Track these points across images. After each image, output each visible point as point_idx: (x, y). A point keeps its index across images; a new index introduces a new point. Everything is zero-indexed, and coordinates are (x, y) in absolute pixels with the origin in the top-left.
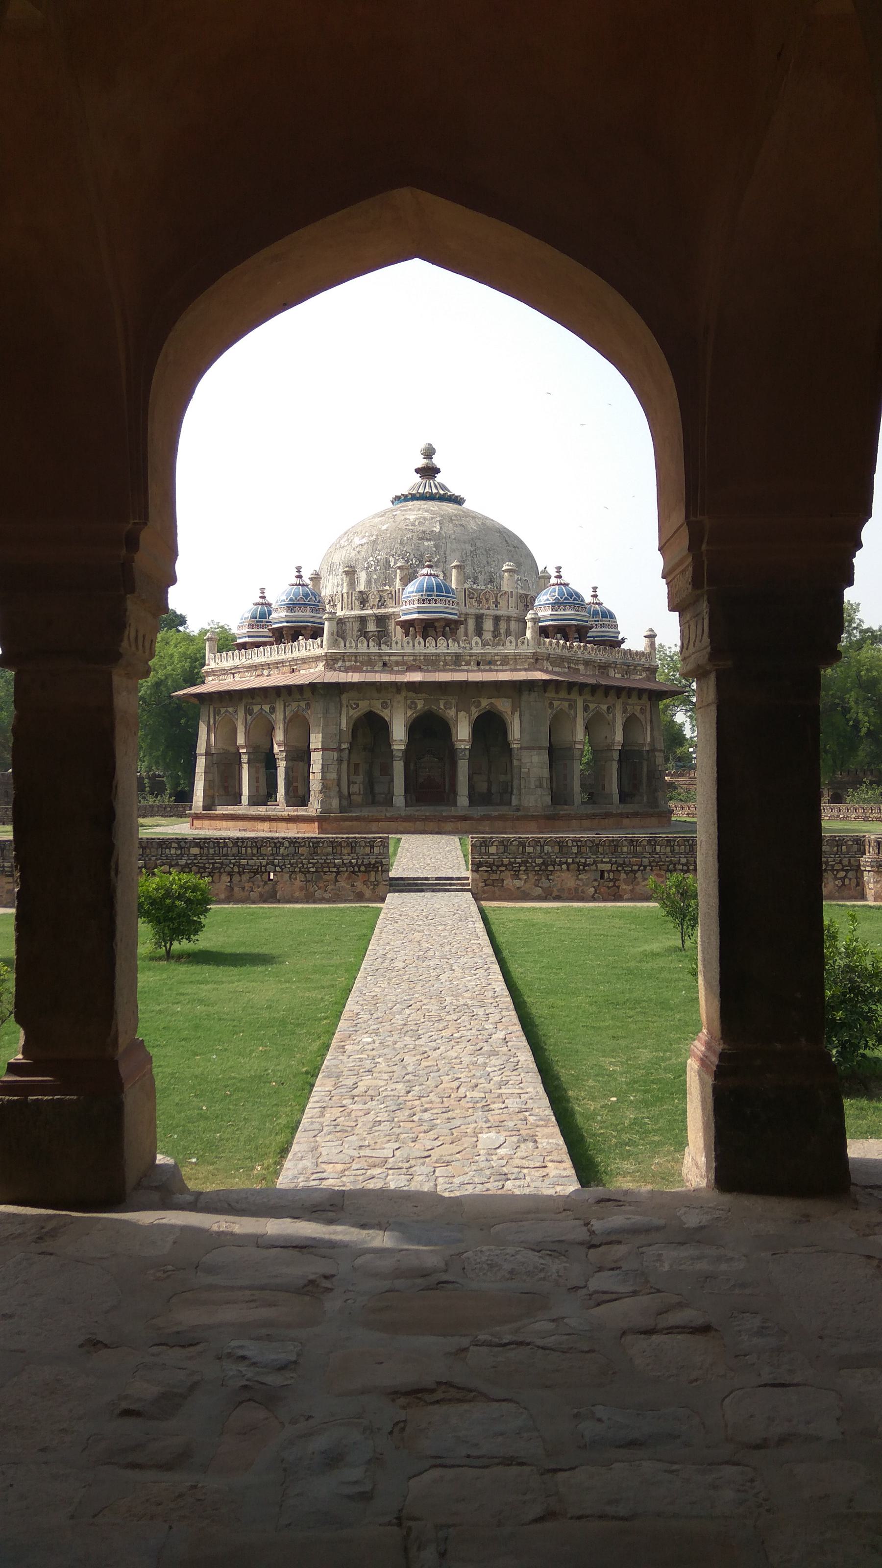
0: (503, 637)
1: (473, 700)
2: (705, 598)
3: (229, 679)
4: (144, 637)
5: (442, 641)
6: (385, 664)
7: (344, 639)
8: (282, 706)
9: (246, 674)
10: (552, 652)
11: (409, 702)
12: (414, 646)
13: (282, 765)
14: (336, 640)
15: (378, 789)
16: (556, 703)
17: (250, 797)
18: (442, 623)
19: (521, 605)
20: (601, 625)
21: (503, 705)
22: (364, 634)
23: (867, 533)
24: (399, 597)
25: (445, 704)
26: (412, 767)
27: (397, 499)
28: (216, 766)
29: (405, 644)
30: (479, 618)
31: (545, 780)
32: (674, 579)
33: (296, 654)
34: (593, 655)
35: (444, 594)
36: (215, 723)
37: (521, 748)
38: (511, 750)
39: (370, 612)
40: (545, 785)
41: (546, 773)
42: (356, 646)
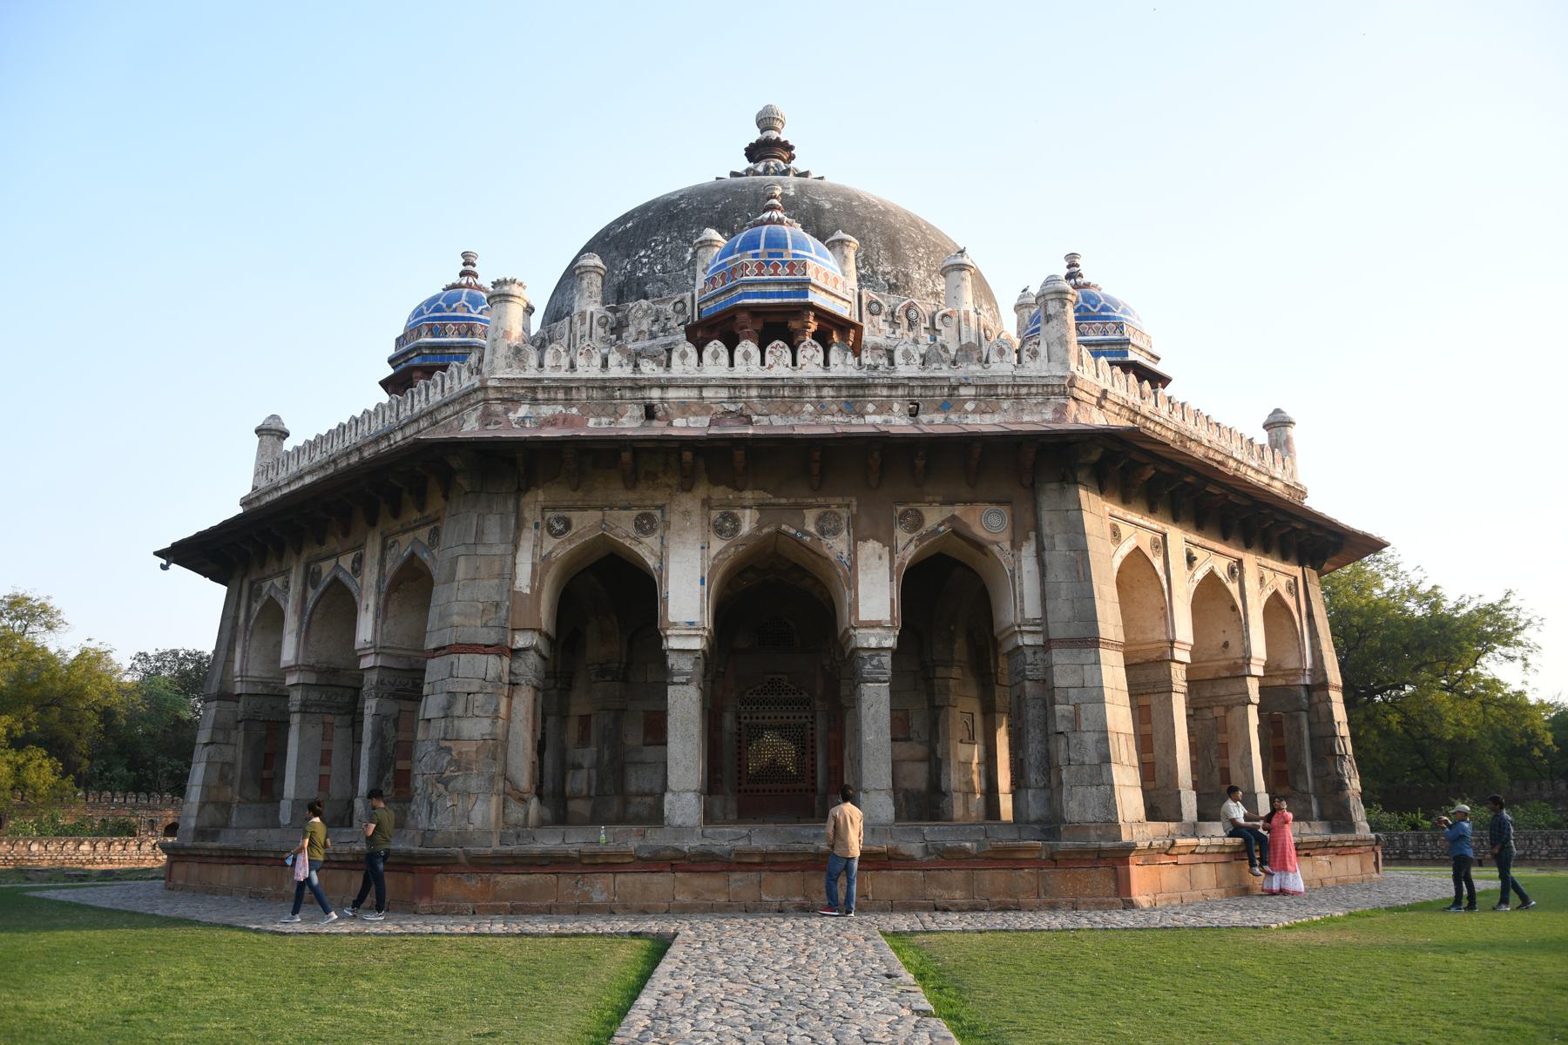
1: (901, 509)
5: (810, 354)
6: (650, 413)
8: (378, 548)
10: (1107, 386)
11: (715, 514)
12: (732, 364)
13: (370, 706)
15: (637, 781)
25: (820, 520)
26: (729, 722)
28: (241, 726)
29: (706, 354)
31: (1122, 738)
35: (813, 255)
37: (1047, 646)
40: (1124, 758)
42: (572, 366)
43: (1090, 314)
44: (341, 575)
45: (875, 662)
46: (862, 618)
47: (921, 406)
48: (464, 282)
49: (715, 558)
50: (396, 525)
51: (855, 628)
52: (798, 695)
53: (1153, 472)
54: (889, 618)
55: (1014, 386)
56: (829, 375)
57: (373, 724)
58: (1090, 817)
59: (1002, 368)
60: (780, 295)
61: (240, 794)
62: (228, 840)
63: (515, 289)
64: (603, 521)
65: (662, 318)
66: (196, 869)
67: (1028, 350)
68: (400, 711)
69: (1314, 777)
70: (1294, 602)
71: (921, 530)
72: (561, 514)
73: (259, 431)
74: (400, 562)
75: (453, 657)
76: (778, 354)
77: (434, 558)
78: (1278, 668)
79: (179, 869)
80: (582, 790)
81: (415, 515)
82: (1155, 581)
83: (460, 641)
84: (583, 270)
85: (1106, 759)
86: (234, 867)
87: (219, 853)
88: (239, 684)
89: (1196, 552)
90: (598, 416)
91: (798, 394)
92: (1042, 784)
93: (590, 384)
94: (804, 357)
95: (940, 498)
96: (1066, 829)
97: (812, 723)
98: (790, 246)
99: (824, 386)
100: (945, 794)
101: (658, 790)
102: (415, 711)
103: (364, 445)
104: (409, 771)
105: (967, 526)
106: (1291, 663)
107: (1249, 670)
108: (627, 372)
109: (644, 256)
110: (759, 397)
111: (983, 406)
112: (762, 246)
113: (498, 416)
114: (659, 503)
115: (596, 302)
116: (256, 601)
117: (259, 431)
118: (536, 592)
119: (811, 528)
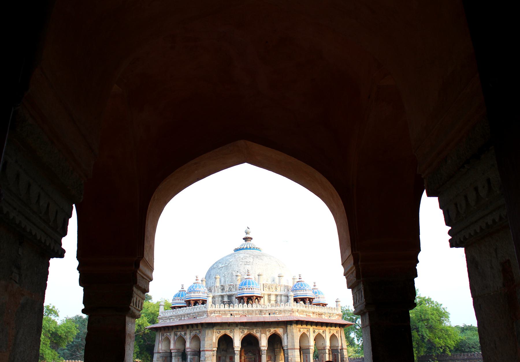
0: (279, 303)
1: (268, 329)
2: (362, 283)
3: (168, 321)
4: (139, 301)
6: (231, 315)
7: (215, 304)
9: (175, 319)
13: (189, 357)
14: (212, 305)
18: (255, 298)
19: (286, 290)
20: (318, 297)
21: (280, 331)
22: (223, 302)
23: (420, 257)
24: (237, 288)
25: (256, 331)
27: (236, 250)
30: (269, 295)
32: (348, 276)
33: (195, 311)
35: (255, 286)
36: (162, 339)
37: (288, 349)
38: (284, 350)
39: (225, 293)
42: (220, 307)
44: (182, 335)
46: (262, 345)
56: (257, 309)
70: (338, 335)
74: (193, 336)
77: (200, 336)
81: (197, 328)
90: (224, 315)
93: (223, 311)
98: (251, 284)
118: (216, 342)
119: (255, 332)
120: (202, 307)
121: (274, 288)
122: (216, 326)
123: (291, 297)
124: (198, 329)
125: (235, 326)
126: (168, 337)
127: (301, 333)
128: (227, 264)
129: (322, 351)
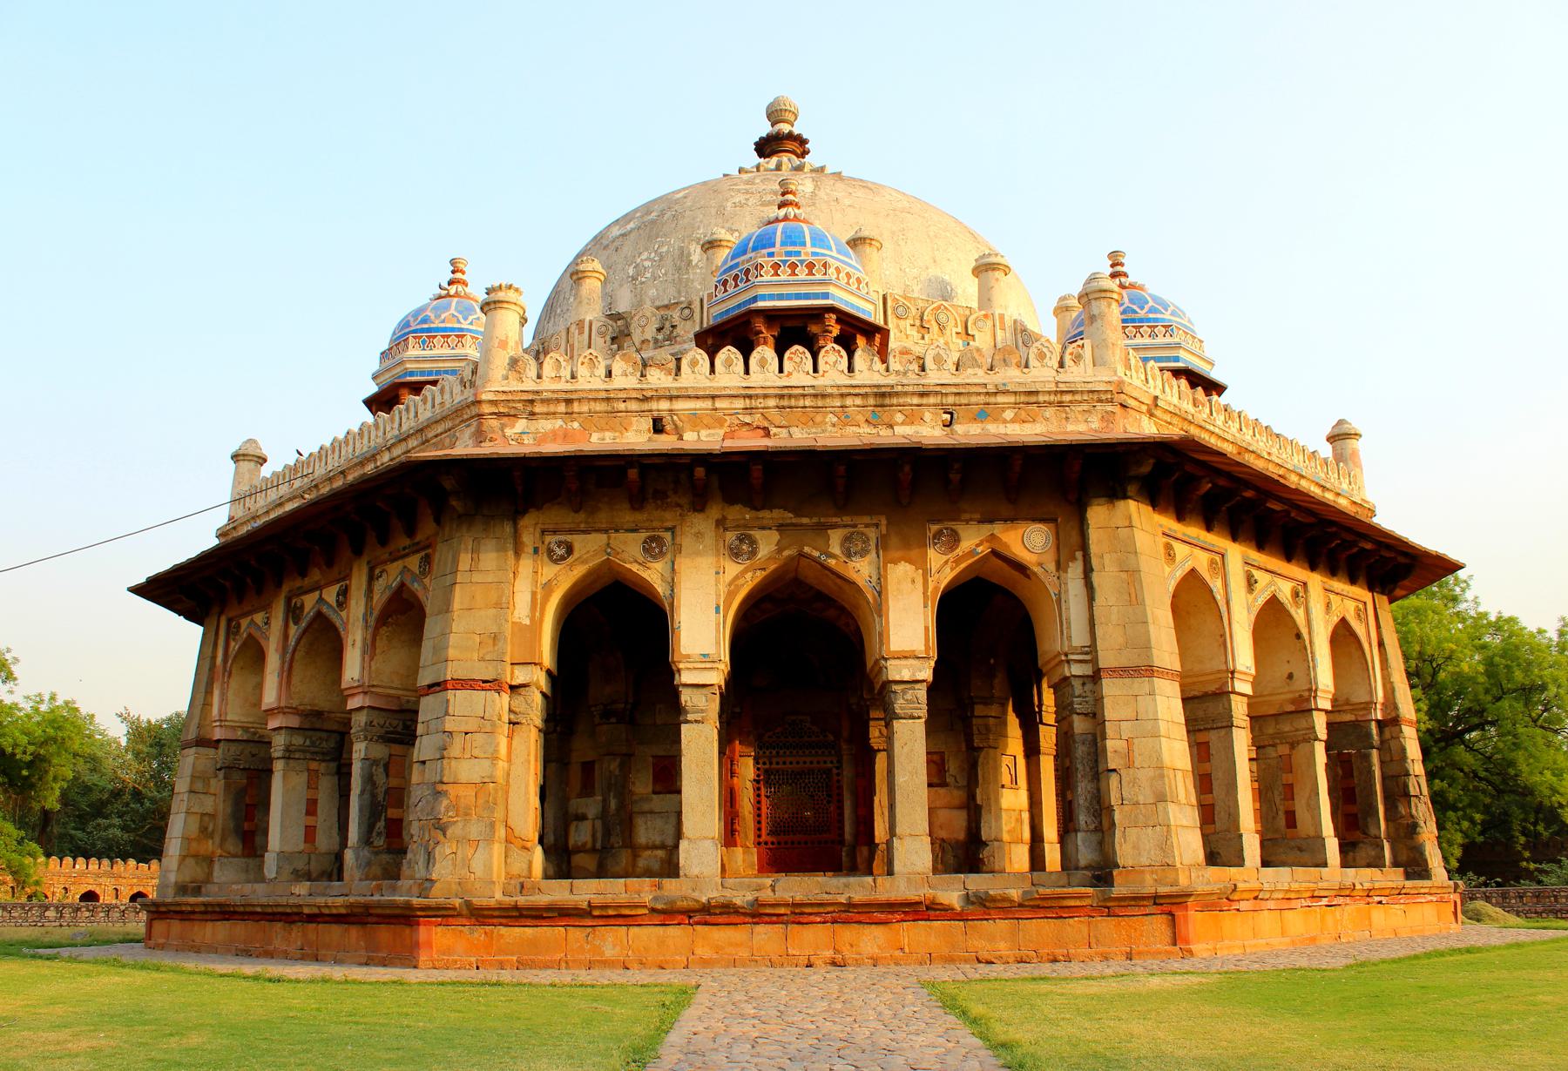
1: (935, 528)
5: (832, 356)
6: (658, 427)
8: (364, 579)
10: (1158, 393)
12: (747, 372)
13: (359, 750)
14: (514, 363)
15: (646, 832)
16: (1180, 549)
17: (281, 854)
28: (221, 774)
31: (1179, 775)
34: (1249, 438)
35: (834, 254)
36: (225, 660)
41: (1176, 751)
43: (1136, 316)
44: (325, 610)
45: (908, 696)
46: (893, 648)
47: (955, 416)
48: (452, 292)
49: (730, 585)
50: (383, 554)
51: (886, 659)
52: (821, 737)
53: (1210, 485)
54: (923, 648)
55: (1056, 393)
56: (854, 382)
57: (362, 769)
58: (1144, 861)
59: (1042, 375)
60: (798, 296)
61: (221, 846)
62: (211, 896)
63: (511, 296)
64: (608, 544)
65: (668, 325)
66: (176, 926)
67: (1071, 354)
68: (390, 755)
69: (1387, 820)
71: (957, 551)
72: (562, 538)
73: (236, 457)
74: (388, 594)
75: (450, 694)
76: (798, 360)
77: (425, 588)
78: (1347, 702)
79: (159, 926)
80: (586, 843)
81: (407, 542)
82: (1213, 605)
83: (455, 677)
84: (580, 275)
85: (1161, 798)
86: (219, 923)
87: (203, 909)
88: (218, 729)
89: (1257, 574)
90: (602, 430)
91: (820, 403)
92: (1092, 827)
94: (826, 363)
95: (978, 516)
96: (1120, 874)
97: (838, 768)
99: (850, 394)
100: (985, 844)
101: (670, 842)
102: (406, 757)
103: (349, 469)
104: (400, 821)
105: (1006, 546)
106: (1360, 697)
107: (1316, 703)
108: (631, 382)
109: (648, 259)
110: (778, 407)
111: (1023, 415)
112: (778, 245)
113: (493, 432)
114: (669, 524)
115: (594, 310)
116: (234, 640)
117: (236, 457)
120: (447, 388)
121: (953, 329)
122: (539, 508)
123: (1103, 303)
124: (416, 541)
125: (679, 505)
126: (257, 634)
127: (1179, 574)
128: (654, 214)
129: (1286, 727)
